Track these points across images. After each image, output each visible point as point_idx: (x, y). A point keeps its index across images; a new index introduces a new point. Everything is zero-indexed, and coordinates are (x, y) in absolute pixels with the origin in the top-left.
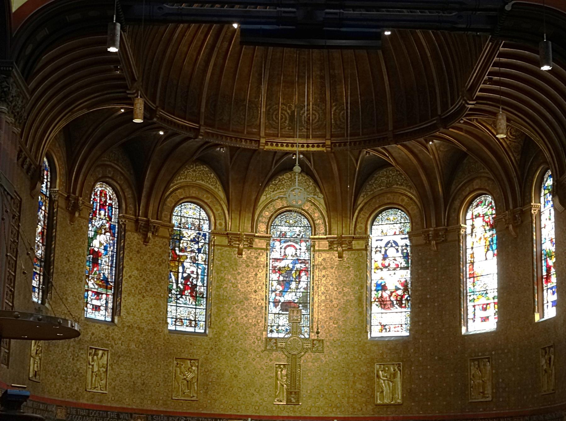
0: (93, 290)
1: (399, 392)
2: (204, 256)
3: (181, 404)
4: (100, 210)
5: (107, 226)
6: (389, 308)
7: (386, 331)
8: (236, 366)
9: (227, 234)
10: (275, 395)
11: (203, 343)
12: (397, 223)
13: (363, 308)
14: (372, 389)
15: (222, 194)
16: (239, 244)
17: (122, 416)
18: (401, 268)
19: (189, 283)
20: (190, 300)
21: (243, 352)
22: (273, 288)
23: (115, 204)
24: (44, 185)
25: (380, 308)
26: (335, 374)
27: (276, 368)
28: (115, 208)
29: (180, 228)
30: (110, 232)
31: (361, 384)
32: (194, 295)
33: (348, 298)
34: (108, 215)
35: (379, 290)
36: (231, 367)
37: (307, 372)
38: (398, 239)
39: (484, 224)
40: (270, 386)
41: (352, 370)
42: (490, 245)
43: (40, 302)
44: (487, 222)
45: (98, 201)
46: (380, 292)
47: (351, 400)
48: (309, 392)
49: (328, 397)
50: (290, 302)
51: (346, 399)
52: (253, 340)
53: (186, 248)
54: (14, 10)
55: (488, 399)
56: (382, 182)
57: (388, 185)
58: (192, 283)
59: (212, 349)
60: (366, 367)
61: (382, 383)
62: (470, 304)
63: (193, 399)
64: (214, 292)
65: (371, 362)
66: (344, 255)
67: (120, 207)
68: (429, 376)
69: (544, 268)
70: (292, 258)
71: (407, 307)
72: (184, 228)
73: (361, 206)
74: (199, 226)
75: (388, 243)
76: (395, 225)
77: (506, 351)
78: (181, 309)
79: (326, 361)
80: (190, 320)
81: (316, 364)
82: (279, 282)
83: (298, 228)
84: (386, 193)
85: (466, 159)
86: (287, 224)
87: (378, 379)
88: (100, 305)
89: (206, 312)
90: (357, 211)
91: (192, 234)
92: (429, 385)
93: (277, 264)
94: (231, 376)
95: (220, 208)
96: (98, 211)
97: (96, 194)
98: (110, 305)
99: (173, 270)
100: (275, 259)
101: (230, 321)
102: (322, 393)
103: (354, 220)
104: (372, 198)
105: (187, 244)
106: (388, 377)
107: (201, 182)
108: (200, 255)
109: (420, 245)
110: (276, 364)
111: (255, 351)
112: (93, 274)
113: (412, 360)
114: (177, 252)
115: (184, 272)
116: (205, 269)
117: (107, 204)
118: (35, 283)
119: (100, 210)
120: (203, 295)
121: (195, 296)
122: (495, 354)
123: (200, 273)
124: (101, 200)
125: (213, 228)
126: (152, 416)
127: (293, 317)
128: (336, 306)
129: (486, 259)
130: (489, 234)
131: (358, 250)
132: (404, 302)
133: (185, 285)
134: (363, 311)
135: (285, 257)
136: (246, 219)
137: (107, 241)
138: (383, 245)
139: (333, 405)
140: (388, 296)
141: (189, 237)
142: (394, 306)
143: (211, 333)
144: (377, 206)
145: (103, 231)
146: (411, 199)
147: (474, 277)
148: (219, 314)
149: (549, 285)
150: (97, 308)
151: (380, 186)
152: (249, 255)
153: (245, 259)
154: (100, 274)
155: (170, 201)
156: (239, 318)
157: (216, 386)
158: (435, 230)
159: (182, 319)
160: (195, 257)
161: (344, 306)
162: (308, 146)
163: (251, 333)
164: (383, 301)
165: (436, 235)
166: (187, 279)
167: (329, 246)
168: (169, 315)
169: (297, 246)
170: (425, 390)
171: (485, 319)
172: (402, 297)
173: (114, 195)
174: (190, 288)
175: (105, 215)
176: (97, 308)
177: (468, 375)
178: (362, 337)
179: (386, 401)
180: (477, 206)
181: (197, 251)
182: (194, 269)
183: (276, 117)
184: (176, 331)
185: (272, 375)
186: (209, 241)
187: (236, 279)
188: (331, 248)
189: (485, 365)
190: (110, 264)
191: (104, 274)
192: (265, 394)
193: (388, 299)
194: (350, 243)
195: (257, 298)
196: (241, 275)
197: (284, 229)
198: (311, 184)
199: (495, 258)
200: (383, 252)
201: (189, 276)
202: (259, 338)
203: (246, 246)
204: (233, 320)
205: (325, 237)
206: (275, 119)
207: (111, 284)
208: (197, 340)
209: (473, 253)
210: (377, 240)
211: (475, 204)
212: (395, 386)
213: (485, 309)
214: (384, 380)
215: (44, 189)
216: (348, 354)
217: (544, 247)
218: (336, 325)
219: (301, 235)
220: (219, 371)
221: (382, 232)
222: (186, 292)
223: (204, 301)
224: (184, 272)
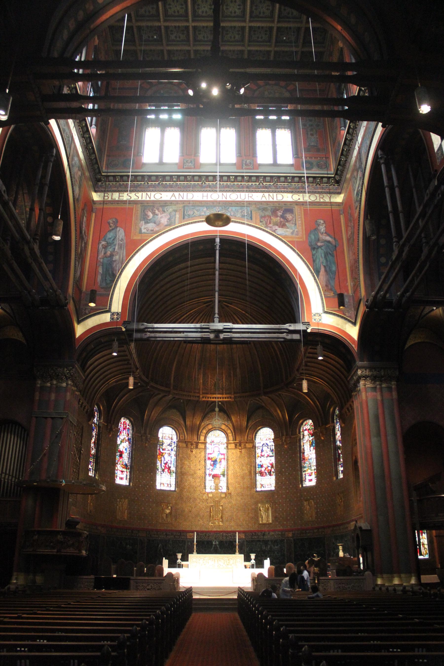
1: (270, 517)
5: (127, 438)
15: (182, 422)
18: (270, 456)
19: (167, 466)
24: (95, 419)
38: (268, 442)
43: (93, 476)
47: (247, 522)
50: (216, 475)
54: (77, 337)
62: (304, 473)
64: (179, 470)
65: (256, 503)
67: (133, 429)
69: (337, 454)
75: (264, 444)
80: (168, 484)
82: (211, 465)
91: (169, 441)
93: (210, 456)
97: (121, 423)
98: (128, 477)
115: (164, 460)
118: (90, 467)
125: (178, 438)
130: (311, 438)
131: (249, 448)
132: (272, 473)
133: (165, 467)
138: (261, 446)
149: (340, 463)
150: (121, 479)
162: (223, 398)
164: (262, 473)
166: (166, 464)
171: (311, 480)
176: (121, 479)
180: (305, 425)
184: (161, 490)
189: (311, 502)
195: (200, 473)
199: (314, 450)
201: (167, 462)
205: (233, 442)
211: (304, 424)
213: (310, 475)
215: (96, 421)
217: (337, 444)
223: (174, 475)
224: (164, 460)
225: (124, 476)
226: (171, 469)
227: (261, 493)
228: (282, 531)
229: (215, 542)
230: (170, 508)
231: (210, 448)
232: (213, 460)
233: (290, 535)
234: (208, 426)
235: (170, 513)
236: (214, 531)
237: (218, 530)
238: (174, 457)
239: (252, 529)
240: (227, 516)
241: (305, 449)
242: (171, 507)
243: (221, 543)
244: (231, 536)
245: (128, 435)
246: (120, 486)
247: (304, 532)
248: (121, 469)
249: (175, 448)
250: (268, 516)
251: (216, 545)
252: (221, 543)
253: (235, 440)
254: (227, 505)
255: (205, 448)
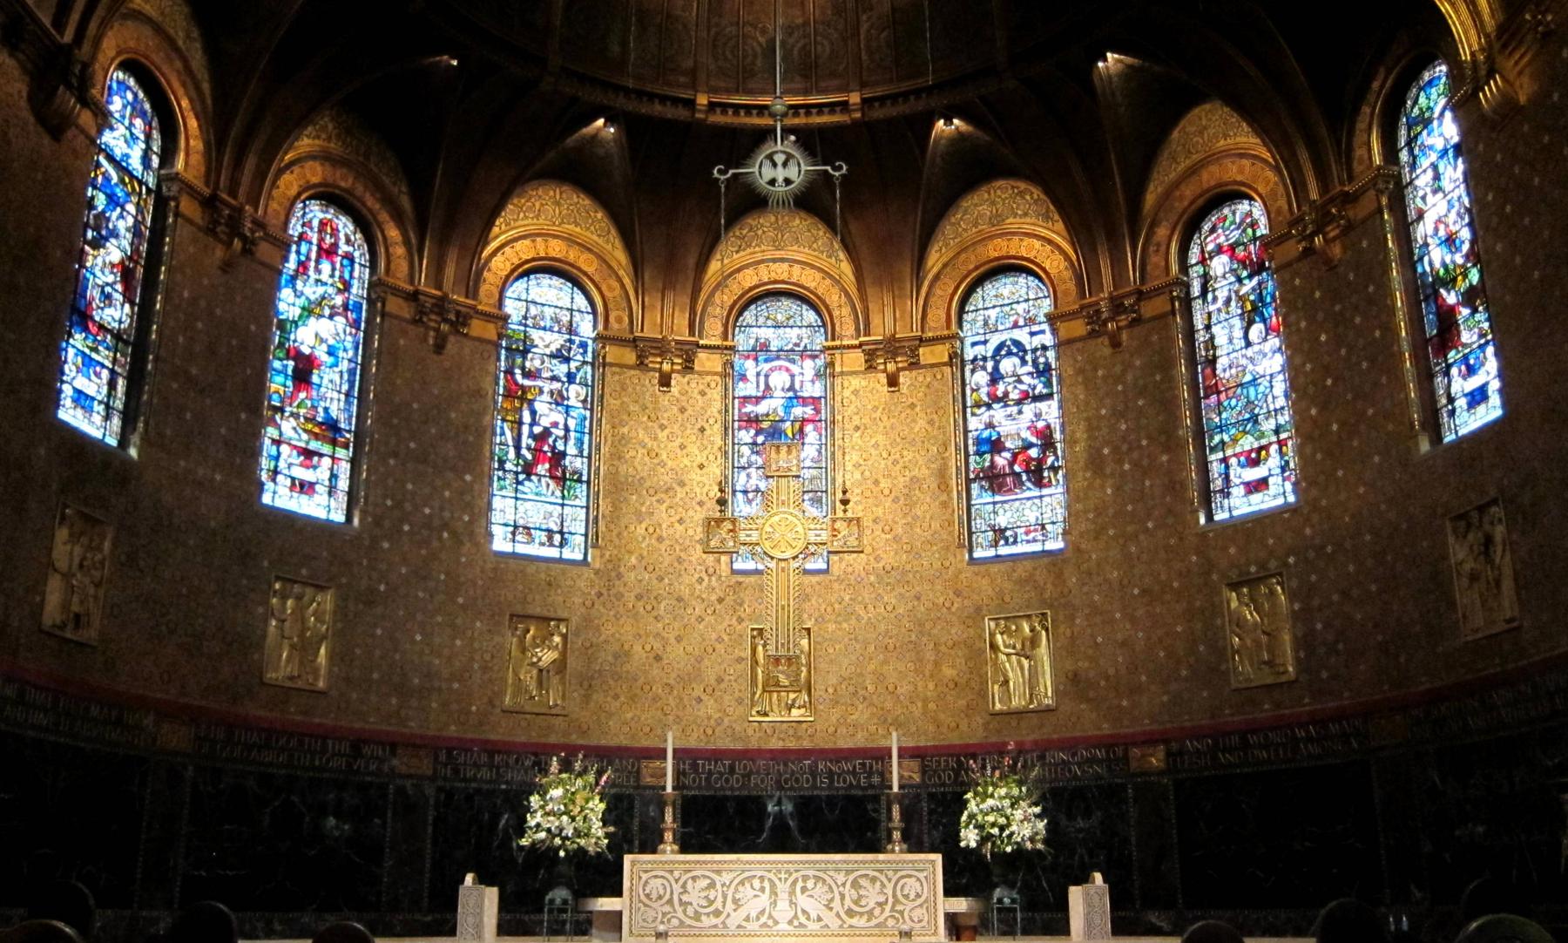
0: (294, 442)
2: (583, 391)
3: (524, 724)
4: (317, 262)
5: (339, 300)
6: (1010, 490)
7: (1007, 543)
8: (658, 634)
9: (635, 340)
10: (752, 700)
11: (578, 582)
12: (1018, 302)
13: (949, 493)
14: (981, 677)
16: (661, 363)
17: (366, 750)
19: (546, 448)
20: (548, 485)
21: (675, 603)
22: (743, 461)
23: (361, 255)
25: (989, 493)
26: (891, 647)
27: (753, 637)
28: (361, 265)
29: (526, 325)
30: (347, 318)
31: (953, 667)
32: (559, 474)
33: (913, 473)
34: (341, 277)
35: (984, 453)
36: (648, 636)
37: (826, 644)
38: (1022, 335)
39: (1235, 266)
40: (740, 680)
41: (929, 635)
42: (1255, 309)
43: (112, 441)
44: (1242, 262)
45: (315, 241)
46: (988, 457)
48: (831, 690)
49: (875, 701)
51: (920, 704)
52: (697, 576)
53: (539, 371)
55: (1284, 679)
56: (981, 215)
57: (997, 219)
58: (553, 448)
59: (600, 595)
60: (962, 627)
61: (1003, 663)
62: (1214, 457)
63: (554, 711)
66: (901, 380)
68: (1119, 637)
70: (783, 394)
71: (1054, 482)
72: (534, 327)
73: (935, 270)
74: (571, 325)
75: (1001, 346)
76: (1014, 306)
77: (1329, 549)
78: (528, 505)
79: (870, 618)
80: (550, 532)
81: (845, 625)
83: (796, 330)
84: (991, 238)
85: (1178, 129)
86: (770, 323)
87: (995, 653)
88: (314, 480)
89: (587, 513)
90: (926, 283)
91: (556, 341)
92: (1120, 659)
94: (647, 658)
95: (616, 285)
96: (312, 264)
98: (343, 484)
99: (509, 418)
100: (745, 398)
101: (643, 531)
102: (861, 692)
103: (921, 302)
104: (959, 253)
105: (543, 362)
106: (1019, 646)
107: (572, 227)
108: (573, 388)
109: (1081, 339)
110: (753, 629)
111: (703, 600)
112: (295, 404)
113: (1077, 602)
114: (519, 378)
115: (533, 423)
116: (585, 418)
117: (340, 252)
119: (317, 262)
120: (581, 475)
121: (561, 477)
122: (1296, 563)
123: (572, 423)
124: (321, 240)
125: (600, 327)
126: (449, 751)
127: (778, 462)
128: (886, 492)
129: (1248, 344)
130: (1249, 285)
131: (933, 366)
132: (1046, 474)
133: (537, 451)
134: (952, 499)
135: (768, 392)
136: (677, 309)
137: (338, 334)
138: (989, 354)
139: (890, 721)
140: (1006, 462)
141: (547, 346)
142: (1022, 484)
143: (598, 559)
144: (971, 267)
145: (327, 312)
146: (1050, 242)
147: (1219, 393)
148: (618, 517)
150: (305, 488)
151: (976, 225)
152: (686, 387)
153: (676, 394)
154: (314, 408)
155: (500, 265)
156: (664, 526)
157: (611, 682)
158: (1112, 299)
159: (529, 528)
160: (560, 392)
161: (906, 491)
163: (693, 559)
164: (998, 476)
165: (1117, 307)
167: (866, 361)
168: (496, 517)
169: (795, 369)
170: (1111, 671)
172: (1040, 461)
173: (359, 236)
174: (550, 460)
175: (332, 276)
176: (305, 488)
177: (1223, 625)
178: (951, 558)
179: (1021, 703)
180: (1213, 230)
181: (565, 379)
182: (560, 419)
183: (732, 52)
184: (514, 555)
185: (743, 655)
186: (594, 358)
187: (656, 439)
188: (870, 367)
189: (1272, 593)
190: (345, 387)
191: (326, 409)
192: (727, 698)
193: (1007, 471)
194: (914, 352)
196: (666, 432)
197: (765, 333)
198: (821, 233)
199: (1274, 342)
200: (990, 370)
201: (546, 433)
202: (711, 571)
203: (679, 367)
204: (651, 530)
205: (857, 342)
206: (730, 56)
207: (348, 436)
208: (564, 574)
209: (1212, 338)
210: (974, 344)
211: (1206, 227)
212: (1036, 667)
213: (1255, 463)
214: (1008, 655)
216: (918, 599)
218: (888, 536)
219: (802, 345)
220: (616, 647)
221: (986, 323)
222: (540, 467)
223: (581, 490)
224: (533, 423)
225: (321, 474)
226: (567, 461)
227: (995, 568)
228: (1109, 743)
229: (779, 803)
230: (557, 639)
231: (751, 375)
232: (765, 425)
233: (1156, 760)
234: (740, 276)
235: (560, 666)
236: (771, 751)
237: (792, 744)
238: (579, 411)
239: (954, 739)
240: (833, 680)
241: (1217, 342)
242: (564, 637)
243: (806, 806)
244: (854, 773)
245: (347, 286)
246: (289, 520)
247: (1235, 740)
248: (302, 440)
249: (589, 369)
250: (1033, 681)
251: (780, 816)
252: (806, 806)
253: (867, 333)
254: (831, 627)
255: (729, 374)
